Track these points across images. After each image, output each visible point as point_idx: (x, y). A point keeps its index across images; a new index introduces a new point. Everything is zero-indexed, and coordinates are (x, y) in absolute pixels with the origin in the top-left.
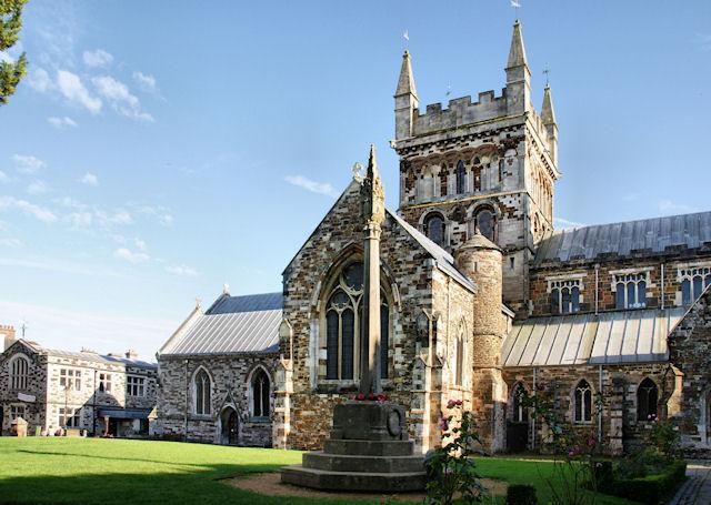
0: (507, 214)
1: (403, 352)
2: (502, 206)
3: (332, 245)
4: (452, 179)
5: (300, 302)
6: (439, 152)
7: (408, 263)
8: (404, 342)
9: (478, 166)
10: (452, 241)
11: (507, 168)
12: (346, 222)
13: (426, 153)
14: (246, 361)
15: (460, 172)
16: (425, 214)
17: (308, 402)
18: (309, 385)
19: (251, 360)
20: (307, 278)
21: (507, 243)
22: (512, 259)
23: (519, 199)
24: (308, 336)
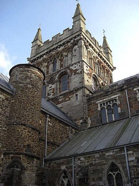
0: (73, 73)
2: (71, 70)
9: (62, 58)
13: (41, 59)
15: (54, 63)
21: (74, 87)
22: (77, 95)
23: (79, 65)
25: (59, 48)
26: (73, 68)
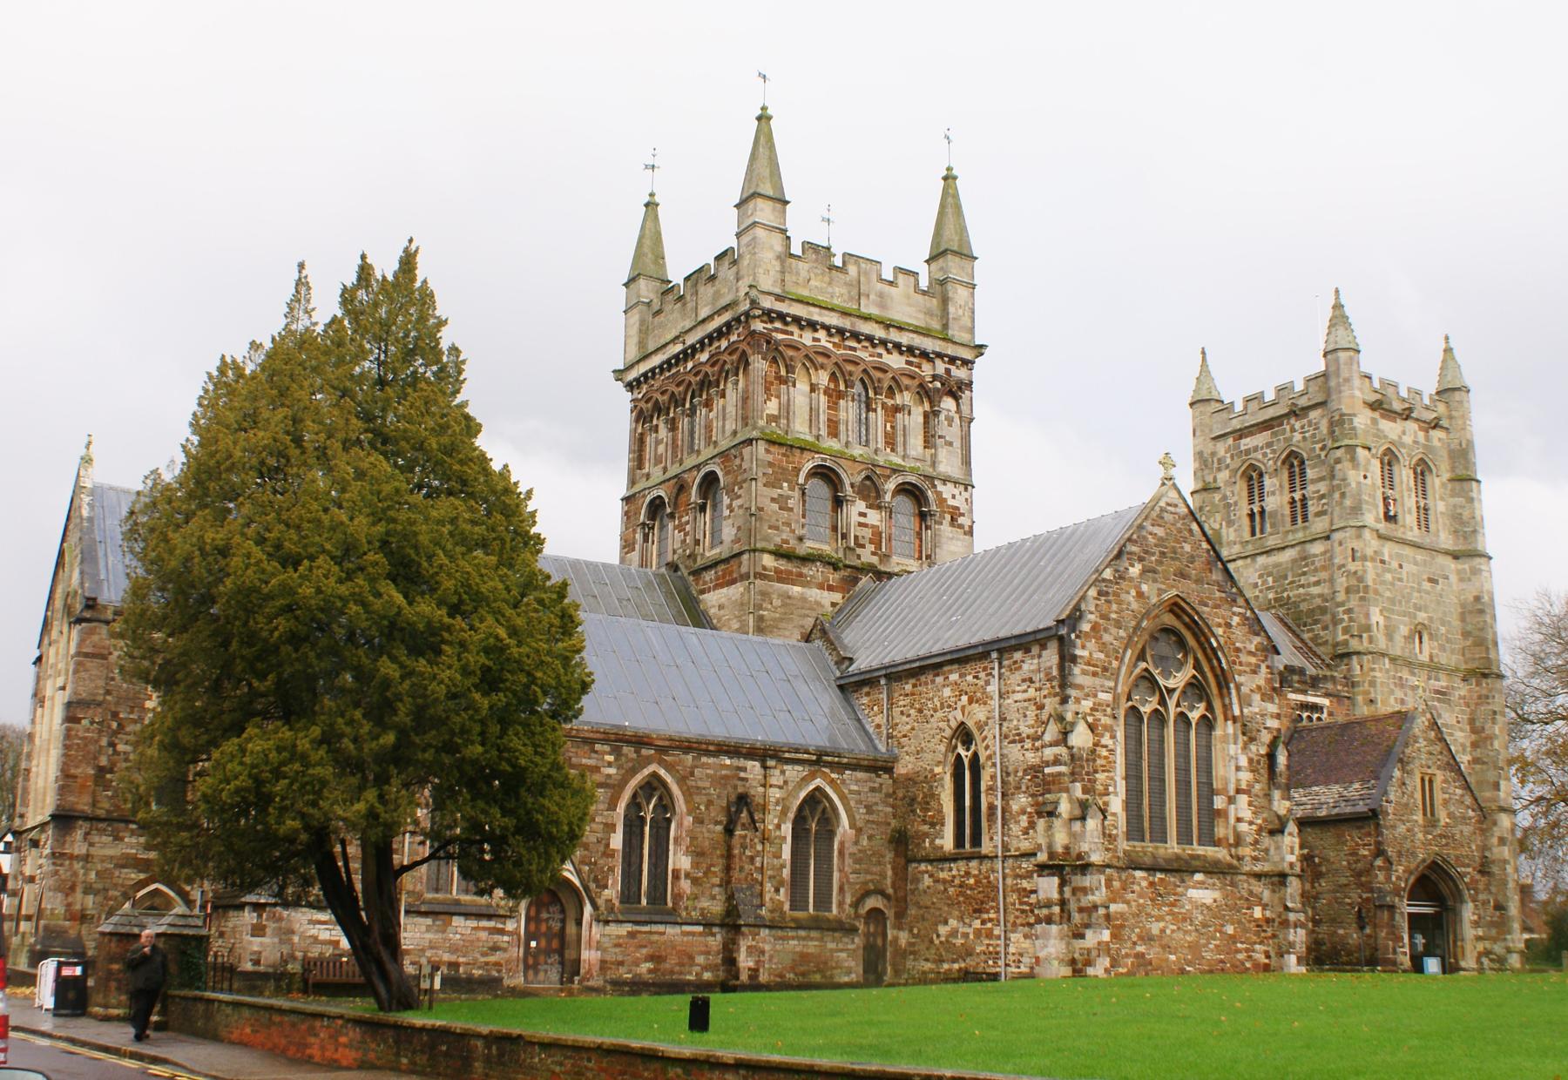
0: (948, 517)
1: (1250, 804)
2: (941, 501)
3: (1145, 588)
4: (849, 411)
5: (1098, 681)
6: (830, 346)
7: (1250, 653)
8: (1250, 786)
10: (856, 537)
11: (943, 428)
13: (807, 338)
14: (616, 751)
16: (810, 465)
17: (1116, 884)
18: (1115, 851)
19: (628, 750)
20: (1107, 638)
24: (1112, 751)
25: (889, 352)
26: (947, 490)
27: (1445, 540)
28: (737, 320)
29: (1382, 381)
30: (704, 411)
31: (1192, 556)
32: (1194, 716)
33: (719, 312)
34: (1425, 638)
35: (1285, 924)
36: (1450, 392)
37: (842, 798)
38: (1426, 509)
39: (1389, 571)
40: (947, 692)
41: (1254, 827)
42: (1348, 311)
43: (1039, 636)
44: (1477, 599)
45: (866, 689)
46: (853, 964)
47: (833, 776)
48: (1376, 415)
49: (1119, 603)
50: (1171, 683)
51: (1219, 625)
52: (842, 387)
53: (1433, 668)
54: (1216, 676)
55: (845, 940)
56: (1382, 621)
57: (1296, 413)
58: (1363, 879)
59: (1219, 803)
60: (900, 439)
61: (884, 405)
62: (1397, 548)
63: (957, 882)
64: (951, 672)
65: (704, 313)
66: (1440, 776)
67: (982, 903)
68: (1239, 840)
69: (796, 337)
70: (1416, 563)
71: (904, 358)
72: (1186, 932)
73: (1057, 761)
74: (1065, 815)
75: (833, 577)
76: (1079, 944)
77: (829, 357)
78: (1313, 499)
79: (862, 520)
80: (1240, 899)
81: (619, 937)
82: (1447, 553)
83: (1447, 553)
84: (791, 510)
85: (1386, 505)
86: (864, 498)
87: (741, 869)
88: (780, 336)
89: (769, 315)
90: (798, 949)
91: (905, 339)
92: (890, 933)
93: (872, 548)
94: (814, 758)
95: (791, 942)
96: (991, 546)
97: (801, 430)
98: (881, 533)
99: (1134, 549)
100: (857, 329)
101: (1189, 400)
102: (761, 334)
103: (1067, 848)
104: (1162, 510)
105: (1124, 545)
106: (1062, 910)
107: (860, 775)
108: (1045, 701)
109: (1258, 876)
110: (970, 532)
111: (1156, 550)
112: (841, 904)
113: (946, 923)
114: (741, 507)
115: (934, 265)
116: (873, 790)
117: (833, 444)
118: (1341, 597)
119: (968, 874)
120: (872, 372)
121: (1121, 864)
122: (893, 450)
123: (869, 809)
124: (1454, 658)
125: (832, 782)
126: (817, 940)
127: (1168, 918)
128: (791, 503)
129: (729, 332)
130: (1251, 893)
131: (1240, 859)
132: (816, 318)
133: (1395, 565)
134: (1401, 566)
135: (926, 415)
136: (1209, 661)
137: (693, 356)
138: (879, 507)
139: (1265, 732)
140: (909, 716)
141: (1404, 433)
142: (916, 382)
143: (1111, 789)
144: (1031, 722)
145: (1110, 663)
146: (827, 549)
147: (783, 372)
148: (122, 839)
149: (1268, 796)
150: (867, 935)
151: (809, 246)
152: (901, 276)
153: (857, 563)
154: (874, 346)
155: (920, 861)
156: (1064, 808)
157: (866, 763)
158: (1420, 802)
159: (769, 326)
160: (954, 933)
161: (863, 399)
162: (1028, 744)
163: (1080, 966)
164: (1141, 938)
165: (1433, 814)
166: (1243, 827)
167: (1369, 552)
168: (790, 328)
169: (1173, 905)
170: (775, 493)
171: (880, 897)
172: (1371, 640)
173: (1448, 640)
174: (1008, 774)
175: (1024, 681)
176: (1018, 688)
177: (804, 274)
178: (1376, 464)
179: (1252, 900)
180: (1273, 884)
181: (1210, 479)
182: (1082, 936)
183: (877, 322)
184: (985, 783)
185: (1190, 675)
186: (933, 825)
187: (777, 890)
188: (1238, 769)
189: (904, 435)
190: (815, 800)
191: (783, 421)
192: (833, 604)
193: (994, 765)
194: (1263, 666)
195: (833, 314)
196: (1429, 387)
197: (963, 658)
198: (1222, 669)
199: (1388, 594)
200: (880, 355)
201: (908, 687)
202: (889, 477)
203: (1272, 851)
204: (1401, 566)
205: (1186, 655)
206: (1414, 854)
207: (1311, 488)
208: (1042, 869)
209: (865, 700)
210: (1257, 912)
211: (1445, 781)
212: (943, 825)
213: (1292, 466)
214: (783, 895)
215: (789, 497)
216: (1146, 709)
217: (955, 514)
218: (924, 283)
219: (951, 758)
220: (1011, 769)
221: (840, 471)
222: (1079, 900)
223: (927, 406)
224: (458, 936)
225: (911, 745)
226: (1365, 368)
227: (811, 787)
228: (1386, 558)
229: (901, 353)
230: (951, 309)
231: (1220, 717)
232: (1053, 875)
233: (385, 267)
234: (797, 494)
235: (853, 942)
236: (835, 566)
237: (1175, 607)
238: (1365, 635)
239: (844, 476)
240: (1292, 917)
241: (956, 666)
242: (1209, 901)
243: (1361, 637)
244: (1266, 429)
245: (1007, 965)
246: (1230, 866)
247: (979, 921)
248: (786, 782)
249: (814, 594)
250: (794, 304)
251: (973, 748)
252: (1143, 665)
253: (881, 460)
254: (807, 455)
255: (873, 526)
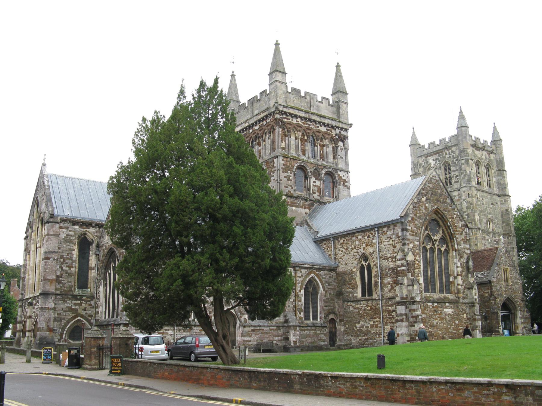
0: (342, 183)
1: (461, 279)
2: (340, 177)
3: (427, 205)
4: (308, 146)
5: (414, 237)
6: (302, 123)
8: (461, 273)
10: (313, 190)
11: (339, 153)
12: (432, 194)
13: (294, 121)
16: (297, 165)
20: (416, 223)
24: (420, 262)
25: (321, 126)
26: (341, 174)
27: (496, 191)
28: (270, 114)
29: (475, 138)
30: (257, 147)
31: (441, 194)
32: (443, 249)
33: (263, 112)
34: (491, 223)
35: (475, 320)
36: (497, 141)
37: (320, 280)
38: (489, 180)
39: (479, 201)
40: (357, 243)
41: (463, 287)
42: (464, 114)
43: (394, 222)
44: (507, 210)
45: (324, 242)
46: (326, 338)
47: (317, 273)
48: (474, 149)
49: (420, 211)
50: (436, 238)
51: (450, 218)
52: (306, 138)
53: (494, 233)
54: (449, 235)
55: (323, 330)
56: (478, 218)
57: (447, 148)
58: (486, 304)
59: (451, 279)
60: (325, 156)
61: (320, 145)
62: (481, 193)
63: (363, 308)
64: (358, 236)
65: (256, 112)
66: (509, 269)
67: (373, 315)
68: (458, 291)
69: (290, 120)
70: (487, 199)
71: (326, 128)
72: (444, 323)
73: (402, 265)
74: (406, 284)
75: (306, 204)
76: (413, 328)
77: (301, 127)
78: (453, 177)
79: (314, 184)
80: (460, 311)
81: (249, 331)
82: (497, 195)
83: (497, 195)
84: (291, 180)
85: (478, 179)
86: (314, 177)
87: (289, 306)
88: (285, 120)
89: (282, 113)
90: (308, 334)
91: (326, 121)
92: (338, 327)
93: (317, 194)
94: (311, 266)
95: (306, 331)
96: (360, 193)
97: (293, 153)
98: (321, 189)
99: (423, 192)
100: (311, 118)
101: (409, 144)
102: (279, 119)
103: (407, 295)
104: (431, 178)
105: (420, 190)
106: (406, 317)
107: (326, 272)
108: (396, 245)
109: (465, 303)
110: (349, 188)
111: (430, 192)
112: (321, 318)
113: (359, 323)
114: (274, 180)
115: (334, 96)
116: (330, 277)
117: (305, 158)
118: (465, 210)
119: (367, 305)
120: (316, 133)
121: (423, 301)
122: (323, 160)
123: (329, 285)
124: (500, 230)
125: (317, 275)
126: (314, 330)
127: (438, 319)
128: (291, 178)
129: (266, 119)
130: (463, 309)
131: (459, 298)
132: (297, 114)
133: (481, 199)
134: (483, 199)
135: (333, 148)
136: (447, 230)
137: (252, 127)
138: (319, 180)
139: (465, 254)
140: (342, 251)
141: (482, 155)
142: (330, 136)
143: (420, 275)
144: (391, 252)
145: (418, 231)
146: (303, 194)
147: (287, 133)
148: (67, 301)
149: (467, 276)
150: (330, 328)
151: (293, 89)
152: (324, 100)
153: (313, 199)
154: (316, 124)
155: (348, 302)
156: (405, 282)
157: (328, 268)
158: (503, 277)
159: (281, 116)
160: (363, 326)
161: (313, 142)
162: (390, 260)
163: (413, 336)
164: (430, 326)
165: (507, 282)
166: (460, 287)
167: (474, 195)
168: (288, 117)
169: (440, 314)
170: (286, 175)
171: (334, 315)
172: (475, 224)
173: (498, 224)
174: (382, 271)
175: (388, 238)
176: (385, 241)
177: (292, 98)
178: (474, 165)
179: (464, 311)
180: (469, 306)
181: (417, 171)
182: (414, 326)
183: (317, 115)
184: (373, 273)
185: (441, 235)
186: (353, 289)
187: (300, 313)
188: (457, 267)
189: (327, 155)
190: (311, 281)
191: (287, 150)
192: (306, 213)
193: (377, 267)
194: (464, 232)
195: (302, 112)
196: (489, 139)
197: (363, 231)
198: (451, 233)
199: (479, 209)
200: (318, 127)
201: (342, 241)
202: (323, 169)
203: (469, 295)
204: (483, 199)
205: (439, 228)
206: (502, 295)
207: (453, 173)
208: (398, 304)
209: (324, 246)
210: (465, 316)
211: (510, 271)
212: (357, 289)
213: (446, 166)
214: (302, 315)
215: (291, 176)
216: (428, 247)
217: (344, 182)
218: (331, 103)
219: (360, 266)
220: (384, 269)
221: (307, 167)
222: (412, 314)
223: (334, 145)
224: (195, 333)
225: (343, 261)
226: (470, 133)
227: (310, 277)
228: (478, 197)
229: (325, 126)
230: (341, 111)
231: (451, 250)
232: (403, 305)
233: (210, 83)
234: (293, 175)
235: (325, 331)
236: (306, 200)
237: (437, 212)
238: (473, 223)
239: (308, 169)
240: (477, 317)
241: (360, 233)
242: (450, 313)
243: (472, 223)
244: (436, 154)
245: (384, 337)
246: (456, 300)
247: (372, 322)
248: (302, 275)
249: (300, 210)
250: (290, 109)
251: (368, 262)
252: (427, 232)
253: (320, 163)
254: (296, 161)
255: (318, 186)
